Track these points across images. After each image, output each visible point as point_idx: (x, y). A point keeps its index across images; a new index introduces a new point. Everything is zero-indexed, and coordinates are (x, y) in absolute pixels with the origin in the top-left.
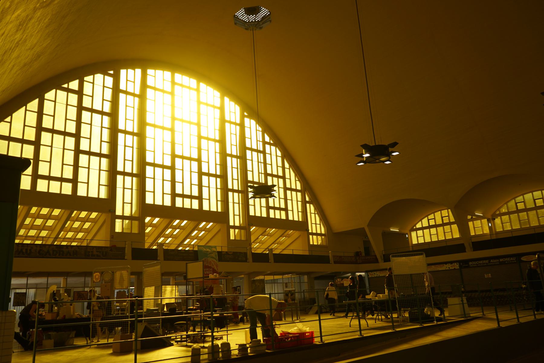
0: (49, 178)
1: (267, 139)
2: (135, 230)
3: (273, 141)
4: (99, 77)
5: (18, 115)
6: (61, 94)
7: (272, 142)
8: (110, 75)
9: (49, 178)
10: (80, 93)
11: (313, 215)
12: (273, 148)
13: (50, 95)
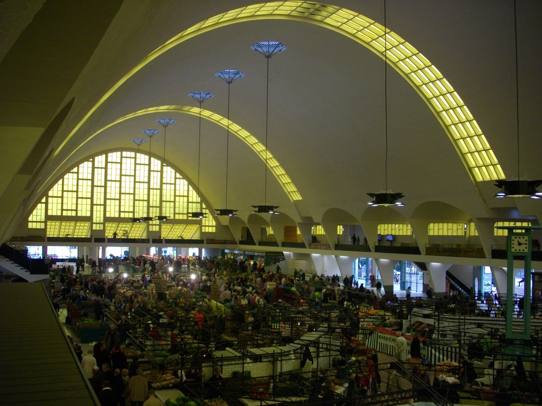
0: (67, 210)
1: (178, 175)
2: (102, 228)
4: (86, 163)
5: (55, 187)
6: (70, 175)
7: (181, 177)
8: (90, 161)
9: (67, 210)
10: (78, 173)
12: (182, 180)
13: (66, 177)
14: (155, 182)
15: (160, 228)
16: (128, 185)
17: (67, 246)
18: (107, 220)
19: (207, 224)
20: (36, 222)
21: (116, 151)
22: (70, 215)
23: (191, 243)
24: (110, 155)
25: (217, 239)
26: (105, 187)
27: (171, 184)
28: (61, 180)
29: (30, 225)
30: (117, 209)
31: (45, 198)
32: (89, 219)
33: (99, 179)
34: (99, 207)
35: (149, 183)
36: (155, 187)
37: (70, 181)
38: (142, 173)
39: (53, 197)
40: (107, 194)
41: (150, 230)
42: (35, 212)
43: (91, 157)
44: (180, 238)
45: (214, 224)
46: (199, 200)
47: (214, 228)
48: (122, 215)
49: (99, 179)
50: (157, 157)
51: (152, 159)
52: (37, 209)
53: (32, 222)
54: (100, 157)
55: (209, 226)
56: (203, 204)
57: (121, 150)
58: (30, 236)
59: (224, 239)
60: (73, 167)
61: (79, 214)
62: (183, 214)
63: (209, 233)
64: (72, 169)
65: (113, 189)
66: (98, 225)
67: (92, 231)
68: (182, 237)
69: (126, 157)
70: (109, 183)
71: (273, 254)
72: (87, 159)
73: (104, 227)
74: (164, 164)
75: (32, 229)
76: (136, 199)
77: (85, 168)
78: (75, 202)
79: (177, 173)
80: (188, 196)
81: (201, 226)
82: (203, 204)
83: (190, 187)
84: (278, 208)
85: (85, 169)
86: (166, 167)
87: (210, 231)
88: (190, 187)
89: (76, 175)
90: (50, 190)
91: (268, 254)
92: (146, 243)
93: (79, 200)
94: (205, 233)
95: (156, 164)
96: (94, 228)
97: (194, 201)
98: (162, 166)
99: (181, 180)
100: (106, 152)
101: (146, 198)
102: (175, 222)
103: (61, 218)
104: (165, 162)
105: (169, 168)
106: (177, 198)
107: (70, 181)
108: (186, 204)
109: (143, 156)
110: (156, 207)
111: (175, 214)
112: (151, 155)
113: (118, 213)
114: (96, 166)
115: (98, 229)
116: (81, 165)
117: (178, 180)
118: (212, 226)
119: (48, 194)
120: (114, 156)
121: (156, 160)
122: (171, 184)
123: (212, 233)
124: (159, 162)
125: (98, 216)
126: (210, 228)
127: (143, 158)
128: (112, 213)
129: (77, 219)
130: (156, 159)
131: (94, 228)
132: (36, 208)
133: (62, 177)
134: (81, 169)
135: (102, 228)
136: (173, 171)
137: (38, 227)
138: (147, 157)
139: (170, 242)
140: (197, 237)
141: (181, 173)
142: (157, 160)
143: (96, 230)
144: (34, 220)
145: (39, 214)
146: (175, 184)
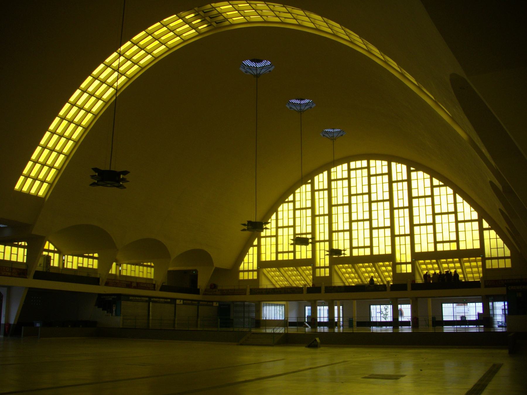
1: (436, 182)
6: (285, 205)
7: (441, 183)
10: (294, 201)
11: (493, 242)
12: (443, 189)
13: (280, 209)
18: (416, 257)
19: (494, 255)
20: (248, 271)
24: (333, 170)
27: (425, 197)
28: (275, 214)
29: (242, 276)
30: (431, 239)
31: (257, 239)
32: (391, 258)
33: (322, 207)
35: (391, 200)
37: (286, 213)
42: (246, 259)
45: (508, 253)
46: (475, 215)
49: (322, 207)
51: (393, 164)
52: (248, 255)
53: (244, 271)
54: (321, 175)
56: (484, 222)
57: (348, 159)
63: (499, 270)
64: (287, 198)
67: (315, 278)
72: (302, 181)
74: (412, 169)
75: (244, 281)
79: (434, 179)
80: (455, 213)
82: (484, 222)
86: (416, 173)
88: (457, 195)
89: (291, 205)
94: (492, 270)
97: (468, 218)
98: (409, 172)
99: (441, 188)
100: (327, 166)
101: (388, 223)
103: (277, 264)
105: (420, 173)
109: (379, 162)
110: (405, 235)
111: (352, 248)
112: (390, 158)
114: (316, 188)
116: (298, 191)
117: (436, 190)
118: (504, 258)
121: (399, 165)
123: (505, 269)
124: (404, 167)
126: (501, 261)
130: (399, 163)
132: (248, 254)
134: (297, 196)
136: (427, 176)
137: (251, 277)
138: (385, 163)
142: (400, 165)
144: (246, 268)
145: (251, 260)
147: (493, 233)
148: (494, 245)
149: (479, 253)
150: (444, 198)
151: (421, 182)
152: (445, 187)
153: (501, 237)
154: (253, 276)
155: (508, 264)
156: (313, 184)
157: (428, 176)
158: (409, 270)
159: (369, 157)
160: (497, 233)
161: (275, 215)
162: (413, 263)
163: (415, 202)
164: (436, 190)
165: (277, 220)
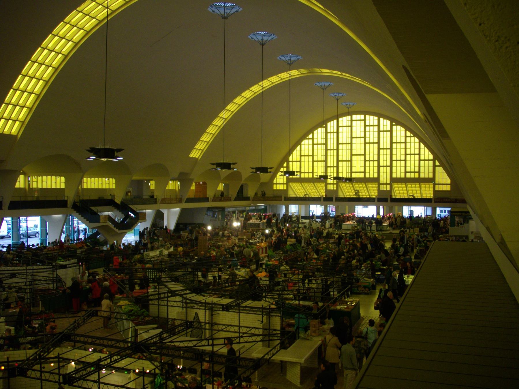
0: (305, 173)
1: (408, 134)
2: (335, 189)
3: (412, 134)
4: (319, 129)
5: (294, 152)
6: (307, 141)
7: (412, 135)
8: (324, 127)
10: (313, 139)
11: (441, 174)
12: (413, 138)
13: (303, 143)
14: (385, 142)
15: (391, 187)
16: (358, 146)
17: (316, 204)
21: (346, 116)
22: (413, 177)
23: (316, 200)
24: (341, 119)
25: (452, 198)
26: (391, 149)
27: (401, 143)
28: (299, 146)
31: (286, 163)
33: (332, 143)
34: (385, 168)
36: (385, 147)
37: (307, 146)
38: (372, 135)
39: (293, 161)
40: (340, 156)
41: (381, 189)
43: (323, 123)
44: (411, 197)
45: (449, 181)
46: (431, 157)
47: (449, 187)
48: (408, 175)
49: (332, 143)
50: (386, 117)
51: (381, 119)
54: (332, 122)
55: (443, 184)
56: (436, 161)
57: (350, 114)
58: (275, 196)
59: (455, 198)
60: (308, 134)
61: (367, 176)
62: (415, 172)
63: (443, 191)
64: (308, 135)
65: (399, 150)
66: (332, 185)
67: (327, 191)
68: (413, 196)
69: (356, 120)
70: (394, 145)
71: (460, 214)
72: (319, 125)
73: (391, 187)
74: (394, 124)
76: (421, 159)
77: (319, 134)
78: (311, 165)
79: (407, 131)
80: (419, 154)
81: (435, 184)
82: (436, 161)
83: (422, 144)
84: (236, 165)
85: (319, 135)
87: (282, 188)
88: (421, 143)
89: (311, 141)
90: (290, 155)
91: (454, 214)
92: (372, 201)
93: (367, 163)
94: (439, 191)
95: (385, 124)
96: (328, 188)
97: (427, 158)
100: (337, 117)
101: (376, 158)
102: (301, 180)
104: (394, 121)
105: (399, 127)
106: (407, 156)
107: (307, 146)
108: (417, 162)
109: (372, 117)
110: (387, 166)
112: (380, 116)
113: (350, 174)
114: (329, 131)
115: (332, 188)
116: (315, 132)
117: (408, 139)
118: (447, 184)
119: (288, 159)
120: (345, 120)
121: (385, 121)
122: (401, 143)
123: (447, 191)
124: (389, 122)
125: (385, 177)
126: (445, 186)
127: (372, 120)
128: (399, 172)
129: (365, 180)
131: (328, 188)
133: (299, 143)
134: (315, 135)
135: (335, 189)
136: (403, 129)
138: (376, 118)
139: (297, 200)
140: (374, 194)
141: (411, 131)
143: (330, 190)
146: (405, 143)
147: (441, 168)
148: (441, 176)
149: (431, 180)
150: (413, 144)
151: (399, 133)
152: (414, 138)
153: (446, 172)
154: (283, 187)
155: (449, 188)
156: (326, 128)
157: (404, 129)
158: (388, 188)
159: (365, 113)
160: (444, 169)
161: (299, 147)
162: (391, 184)
163: (394, 145)
164: (408, 139)
165: (301, 150)
